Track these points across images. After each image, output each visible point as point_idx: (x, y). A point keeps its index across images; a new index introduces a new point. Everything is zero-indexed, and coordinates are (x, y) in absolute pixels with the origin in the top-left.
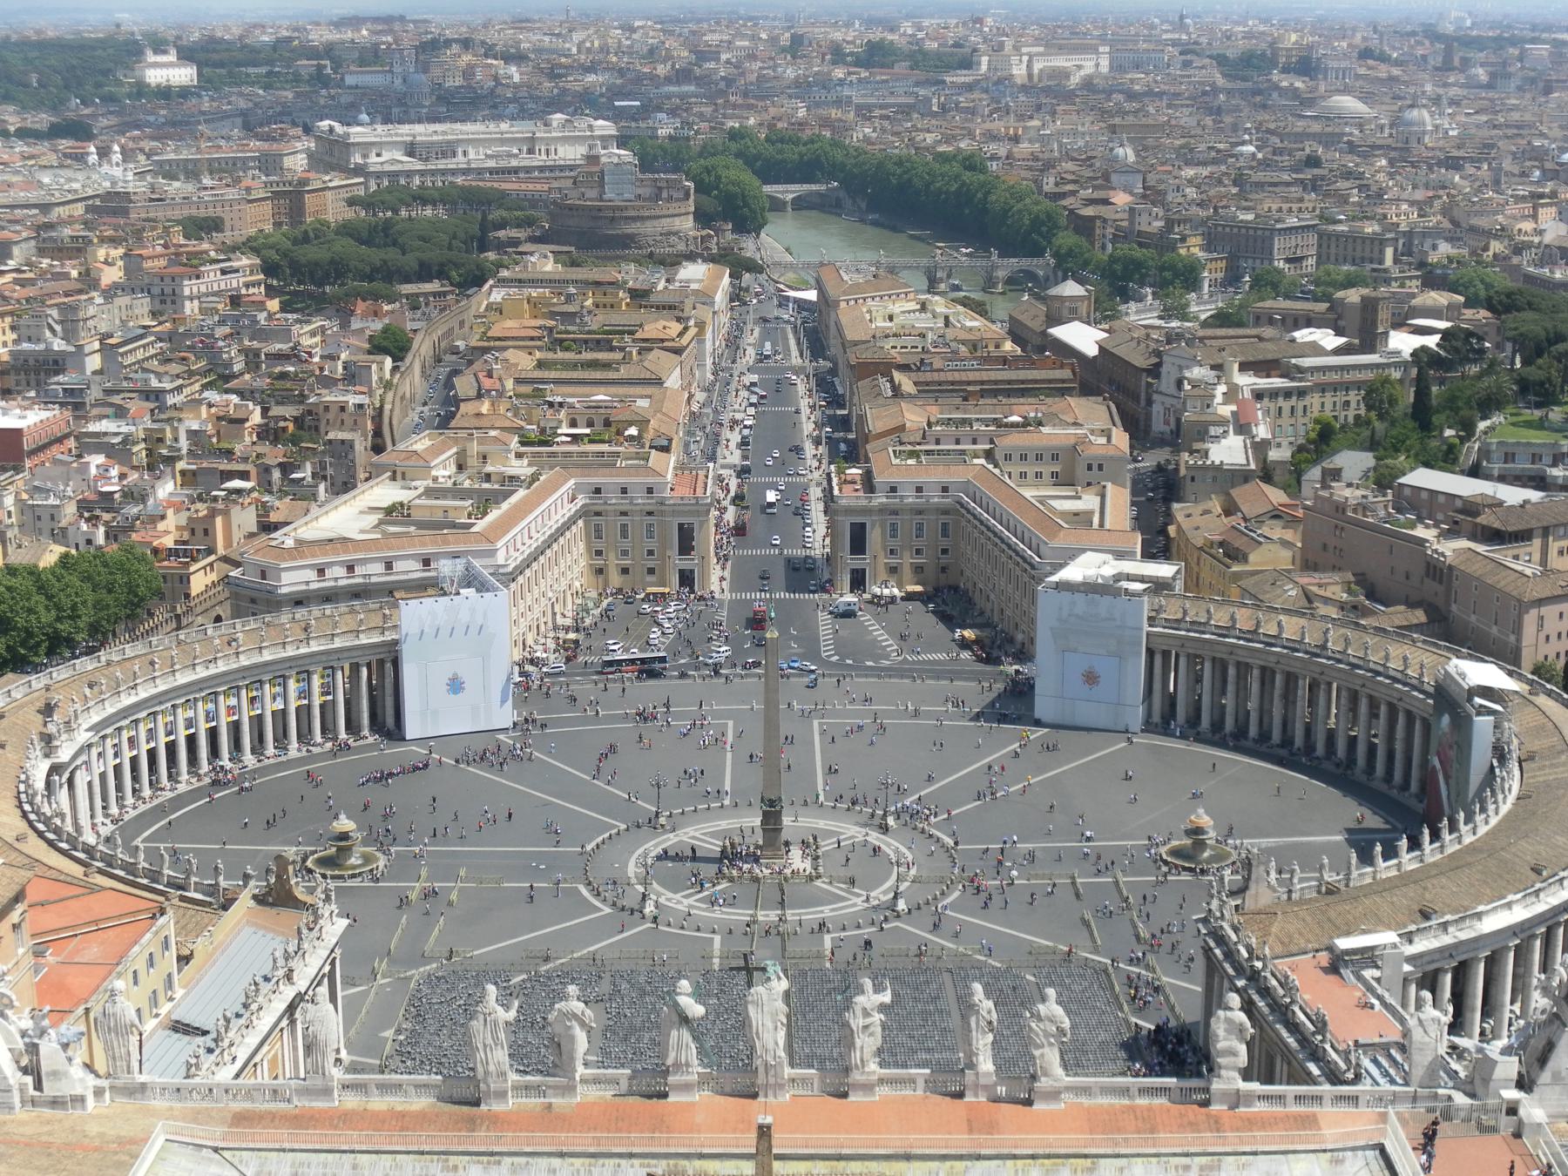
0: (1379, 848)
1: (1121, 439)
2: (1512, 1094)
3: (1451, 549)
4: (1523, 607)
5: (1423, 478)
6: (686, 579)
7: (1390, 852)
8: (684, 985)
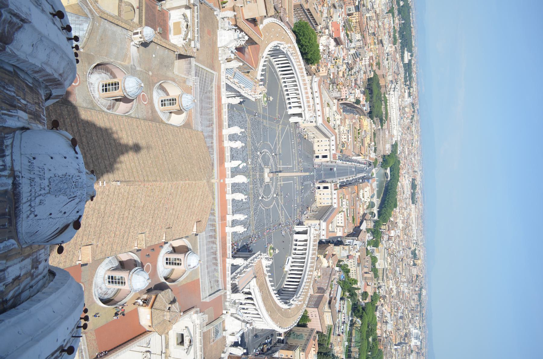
0: (273, 284)
1: (346, 234)
2: (230, 312)
3: (327, 296)
4: (317, 308)
5: (340, 289)
6: (317, 157)
7: (272, 286)
8: (245, 164)
